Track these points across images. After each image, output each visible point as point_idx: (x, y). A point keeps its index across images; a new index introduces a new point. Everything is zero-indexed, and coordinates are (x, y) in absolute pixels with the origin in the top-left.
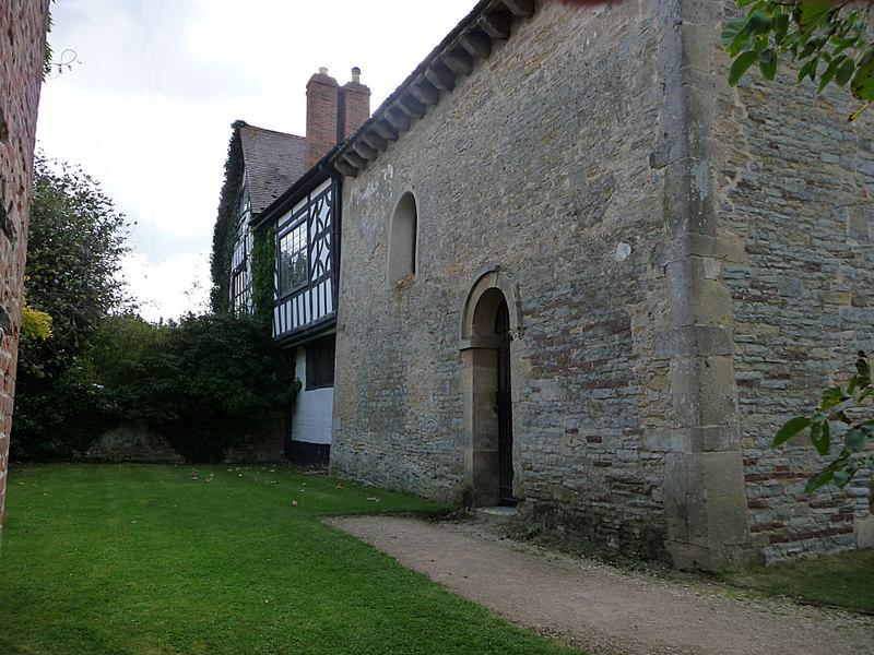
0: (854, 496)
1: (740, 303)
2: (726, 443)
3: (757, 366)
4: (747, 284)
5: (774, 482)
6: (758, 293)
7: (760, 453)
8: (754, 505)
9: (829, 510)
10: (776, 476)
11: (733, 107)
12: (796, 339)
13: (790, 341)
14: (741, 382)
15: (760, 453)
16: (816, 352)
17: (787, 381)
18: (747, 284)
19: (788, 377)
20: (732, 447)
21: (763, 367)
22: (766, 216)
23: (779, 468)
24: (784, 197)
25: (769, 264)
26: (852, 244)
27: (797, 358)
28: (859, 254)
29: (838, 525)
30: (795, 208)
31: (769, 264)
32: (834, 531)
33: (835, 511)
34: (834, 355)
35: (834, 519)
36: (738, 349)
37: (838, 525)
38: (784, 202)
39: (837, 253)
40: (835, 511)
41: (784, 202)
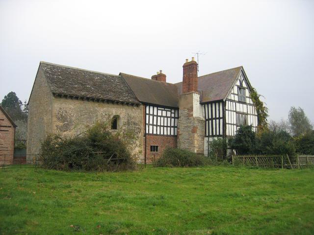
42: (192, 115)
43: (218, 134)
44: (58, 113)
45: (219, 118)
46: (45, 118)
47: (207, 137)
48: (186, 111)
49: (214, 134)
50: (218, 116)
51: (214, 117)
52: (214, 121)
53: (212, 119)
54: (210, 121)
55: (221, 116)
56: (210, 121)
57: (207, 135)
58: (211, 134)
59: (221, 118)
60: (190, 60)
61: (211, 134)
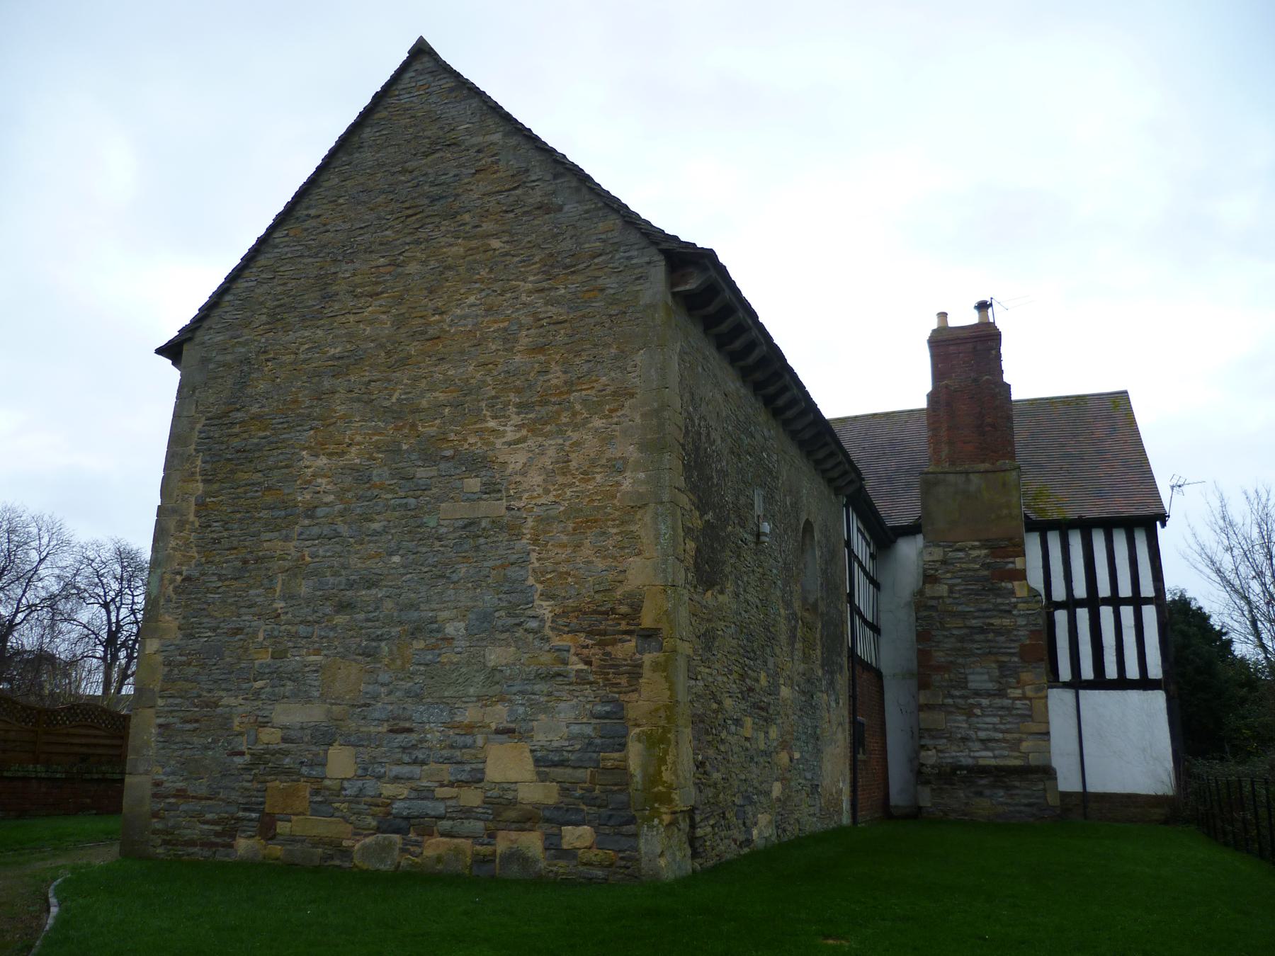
0: (238, 819)
1: (166, 669)
2: (141, 769)
3: (174, 714)
4: (177, 653)
5: (172, 800)
6: (184, 658)
7: (165, 778)
8: (155, 815)
9: (212, 827)
10: (174, 796)
11: (187, 522)
12: (210, 691)
13: (205, 694)
14: (160, 726)
15: (165, 778)
16: (224, 701)
17: (196, 725)
18: (177, 653)
19: (197, 721)
20: (147, 773)
21: (181, 714)
22: (199, 599)
23: (178, 790)
24: (220, 580)
25: (197, 635)
26: (279, 605)
27: (207, 706)
28: (287, 613)
29: (218, 840)
30: (227, 586)
31: (197, 635)
32: (216, 845)
33: (218, 828)
34: (242, 702)
35: (217, 834)
36: (160, 702)
37: (218, 840)
38: (220, 584)
39: (260, 616)
40: (218, 828)
41: (220, 584)
42: (1021, 575)
43: (1133, 672)
44: (687, 432)
45: (1137, 601)
46: (517, 460)
47: (1066, 685)
48: (975, 553)
49: (1111, 672)
50: (1125, 590)
51: (1104, 590)
52: (1106, 613)
53: (1093, 602)
54: (1083, 614)
55: (1147, 590)
56: (1083, 614)
57: (1065, 673)
58: (1087, 673)
59: (1148, 601)
60: (965, 317)
61: (1087, 673)
